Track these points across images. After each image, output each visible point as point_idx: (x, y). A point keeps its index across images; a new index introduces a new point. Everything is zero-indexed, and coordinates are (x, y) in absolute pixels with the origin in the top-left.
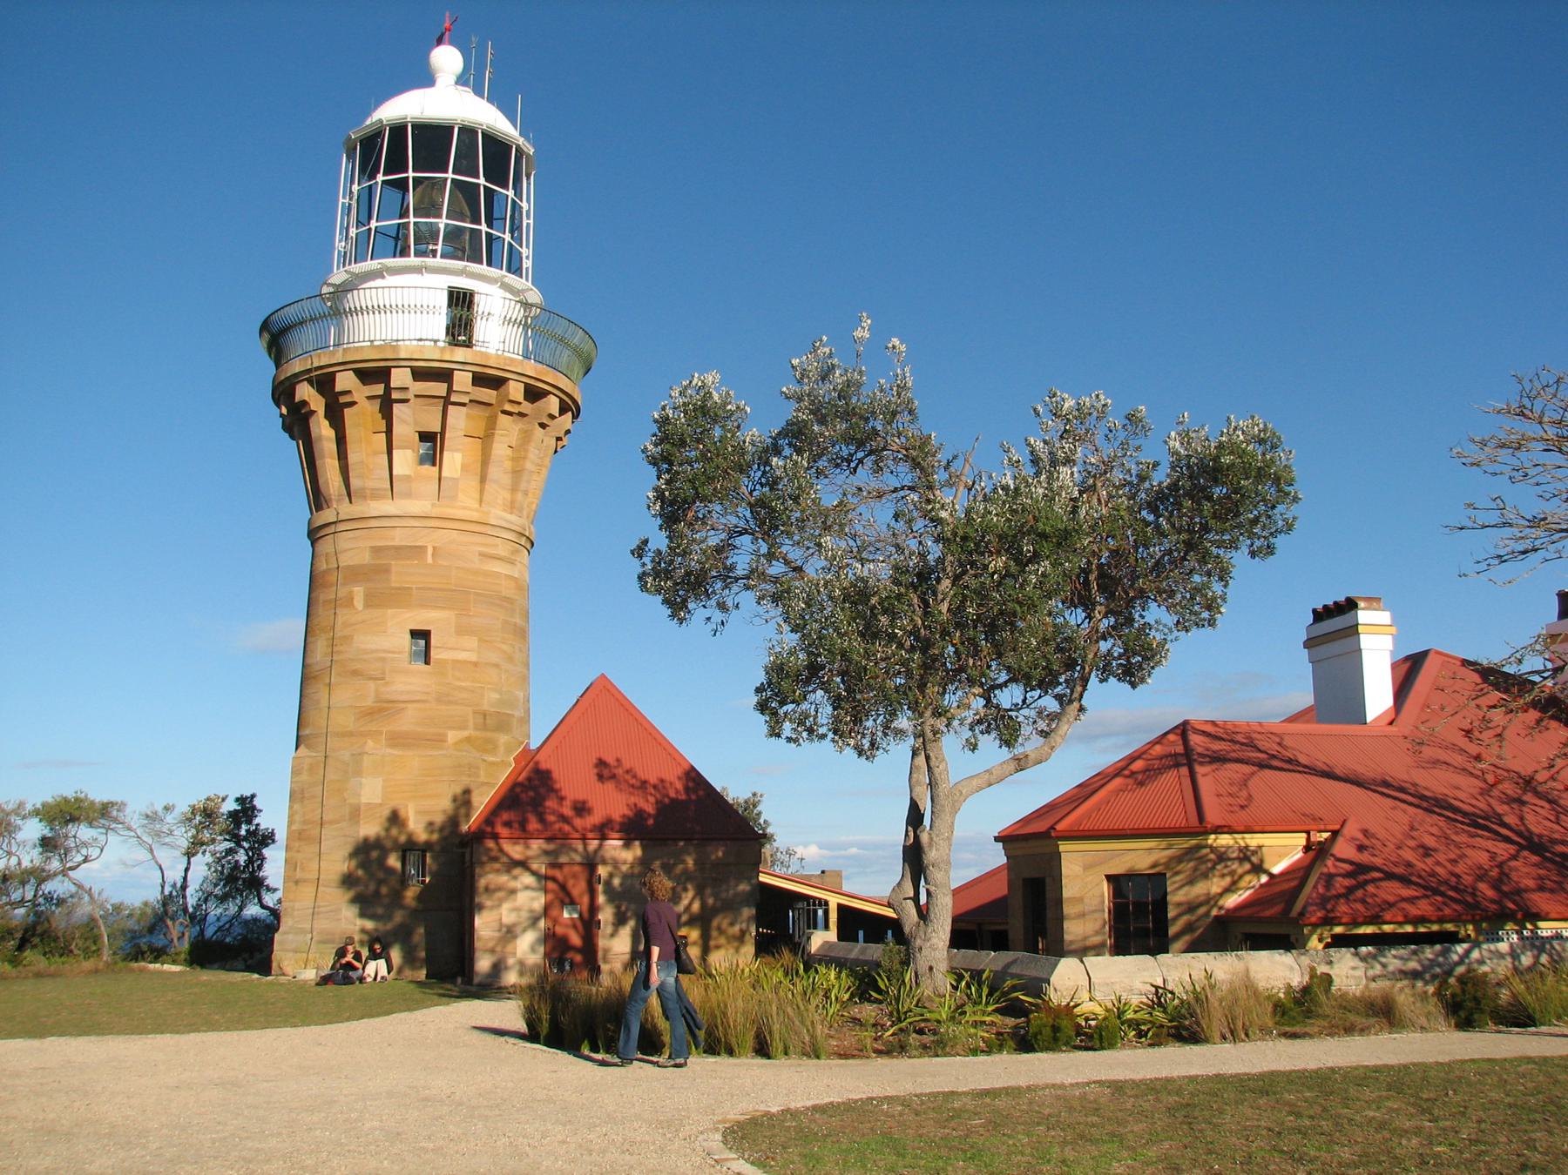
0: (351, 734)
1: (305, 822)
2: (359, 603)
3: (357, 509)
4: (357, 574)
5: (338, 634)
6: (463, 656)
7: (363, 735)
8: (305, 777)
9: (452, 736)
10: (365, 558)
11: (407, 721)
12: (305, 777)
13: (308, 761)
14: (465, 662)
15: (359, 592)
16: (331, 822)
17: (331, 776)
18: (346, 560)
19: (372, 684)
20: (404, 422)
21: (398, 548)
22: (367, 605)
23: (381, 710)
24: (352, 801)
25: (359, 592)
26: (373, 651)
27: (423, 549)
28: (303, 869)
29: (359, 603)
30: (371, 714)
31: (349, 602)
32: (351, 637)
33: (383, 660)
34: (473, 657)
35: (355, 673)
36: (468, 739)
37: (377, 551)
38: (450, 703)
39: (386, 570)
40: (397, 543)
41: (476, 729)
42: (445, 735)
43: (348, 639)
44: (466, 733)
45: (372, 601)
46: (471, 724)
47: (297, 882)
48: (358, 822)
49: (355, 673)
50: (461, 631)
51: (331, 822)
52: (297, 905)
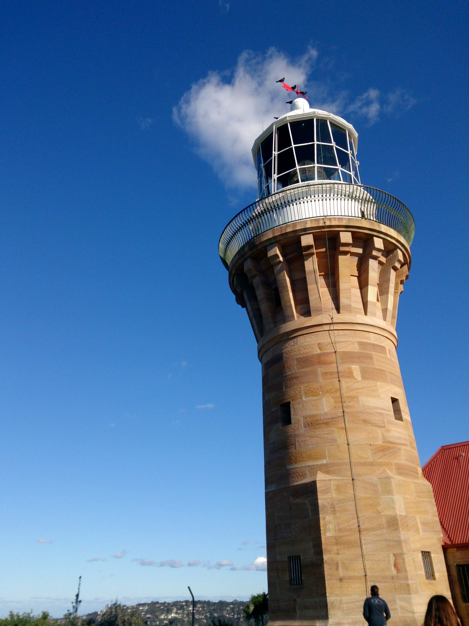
1: (340, 530)
3: (343, 317)
4: (349, 357)
5: (345, 394)
10: (355, 348)
16: (368, 530)
17: (360, 493)
18: (341, 348)
19: (379, 431)
22: (363, 377)
23: (389, 448)
24: (391, 513)
25: (356, 369)
28: (346, 569)
31: (350, 375)
32: (357, 397)
33: (382, 414)
37: (362, 344)
45: (365, 374)
47: (341, 580)
48: (397, 529)
49: (365, 421)
51: (368, 530)
52: (344, 599)
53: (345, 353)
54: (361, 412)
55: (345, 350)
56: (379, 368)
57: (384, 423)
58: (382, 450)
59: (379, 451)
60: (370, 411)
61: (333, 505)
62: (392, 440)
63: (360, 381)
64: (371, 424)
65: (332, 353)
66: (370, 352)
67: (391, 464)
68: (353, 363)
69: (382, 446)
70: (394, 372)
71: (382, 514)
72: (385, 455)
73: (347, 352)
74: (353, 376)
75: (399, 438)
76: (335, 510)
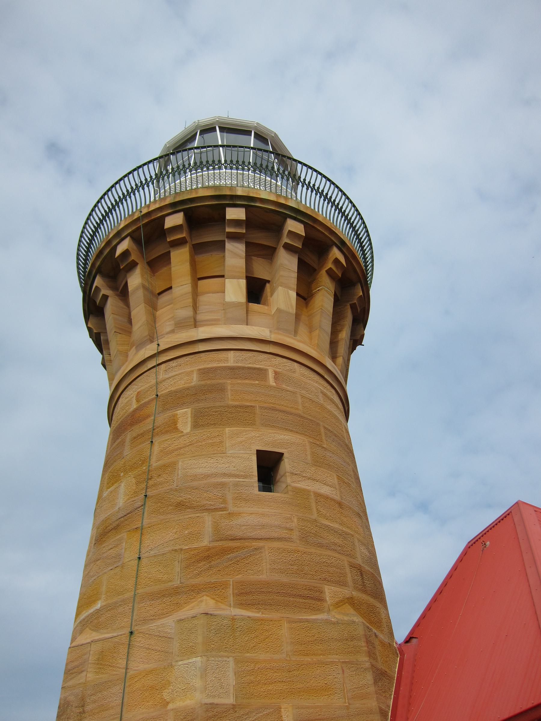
0: (176, 591)
2: (185, 425)
5: (154, 464)
6: (325, 490)
7: (196, 591)
8: (90, 675)
9: (330, 592)
11: (265, 569)
12: (90, 675)
13: (95, 648)
14: (327, 498)
15: (184, 416)
17: (138, 665)
19: (208, 520)
20: (236, 255)
21: (232, 369)
22: (196, 425)
23: (224, 551)
26: (206, 476)
27: (261, 373)
29: (185, 425)
30: (207, 556)
31: (172, 426)
32: (175, 463)
34: (338, 498)
35: (181, 506)
36: (351, 601)
38: (321, 546)
39: (221, 389)
40: (231, 364)
41: (356, 588)
42: (322, 592)
43: (170, 467)
44: (346, 592)
46: (349, 579)
50: (318, 462)
53: (170, 393)
54: (176, 490)
55: (173, 389)
56: (237, 403)
57: (224, 501)
58: (208, 558)
59: (199, 561)
60: (195, 484)
61: (83, 699)
62: (239, 534)
63: (187, 434)
64: (193, 508)
65: (153, 400)
66: (220, 381)
67: (224, 585)
68: (182, 405)
69: (209, 549)
70: (277, 407)
71: (170, 706)
72: (211, 567)
73: (176, 392)
74: (176, 429)
75: (263, 526)
76: (84, 712)
